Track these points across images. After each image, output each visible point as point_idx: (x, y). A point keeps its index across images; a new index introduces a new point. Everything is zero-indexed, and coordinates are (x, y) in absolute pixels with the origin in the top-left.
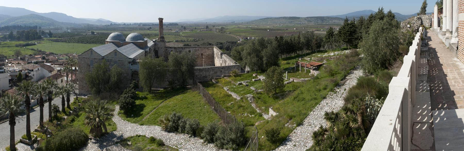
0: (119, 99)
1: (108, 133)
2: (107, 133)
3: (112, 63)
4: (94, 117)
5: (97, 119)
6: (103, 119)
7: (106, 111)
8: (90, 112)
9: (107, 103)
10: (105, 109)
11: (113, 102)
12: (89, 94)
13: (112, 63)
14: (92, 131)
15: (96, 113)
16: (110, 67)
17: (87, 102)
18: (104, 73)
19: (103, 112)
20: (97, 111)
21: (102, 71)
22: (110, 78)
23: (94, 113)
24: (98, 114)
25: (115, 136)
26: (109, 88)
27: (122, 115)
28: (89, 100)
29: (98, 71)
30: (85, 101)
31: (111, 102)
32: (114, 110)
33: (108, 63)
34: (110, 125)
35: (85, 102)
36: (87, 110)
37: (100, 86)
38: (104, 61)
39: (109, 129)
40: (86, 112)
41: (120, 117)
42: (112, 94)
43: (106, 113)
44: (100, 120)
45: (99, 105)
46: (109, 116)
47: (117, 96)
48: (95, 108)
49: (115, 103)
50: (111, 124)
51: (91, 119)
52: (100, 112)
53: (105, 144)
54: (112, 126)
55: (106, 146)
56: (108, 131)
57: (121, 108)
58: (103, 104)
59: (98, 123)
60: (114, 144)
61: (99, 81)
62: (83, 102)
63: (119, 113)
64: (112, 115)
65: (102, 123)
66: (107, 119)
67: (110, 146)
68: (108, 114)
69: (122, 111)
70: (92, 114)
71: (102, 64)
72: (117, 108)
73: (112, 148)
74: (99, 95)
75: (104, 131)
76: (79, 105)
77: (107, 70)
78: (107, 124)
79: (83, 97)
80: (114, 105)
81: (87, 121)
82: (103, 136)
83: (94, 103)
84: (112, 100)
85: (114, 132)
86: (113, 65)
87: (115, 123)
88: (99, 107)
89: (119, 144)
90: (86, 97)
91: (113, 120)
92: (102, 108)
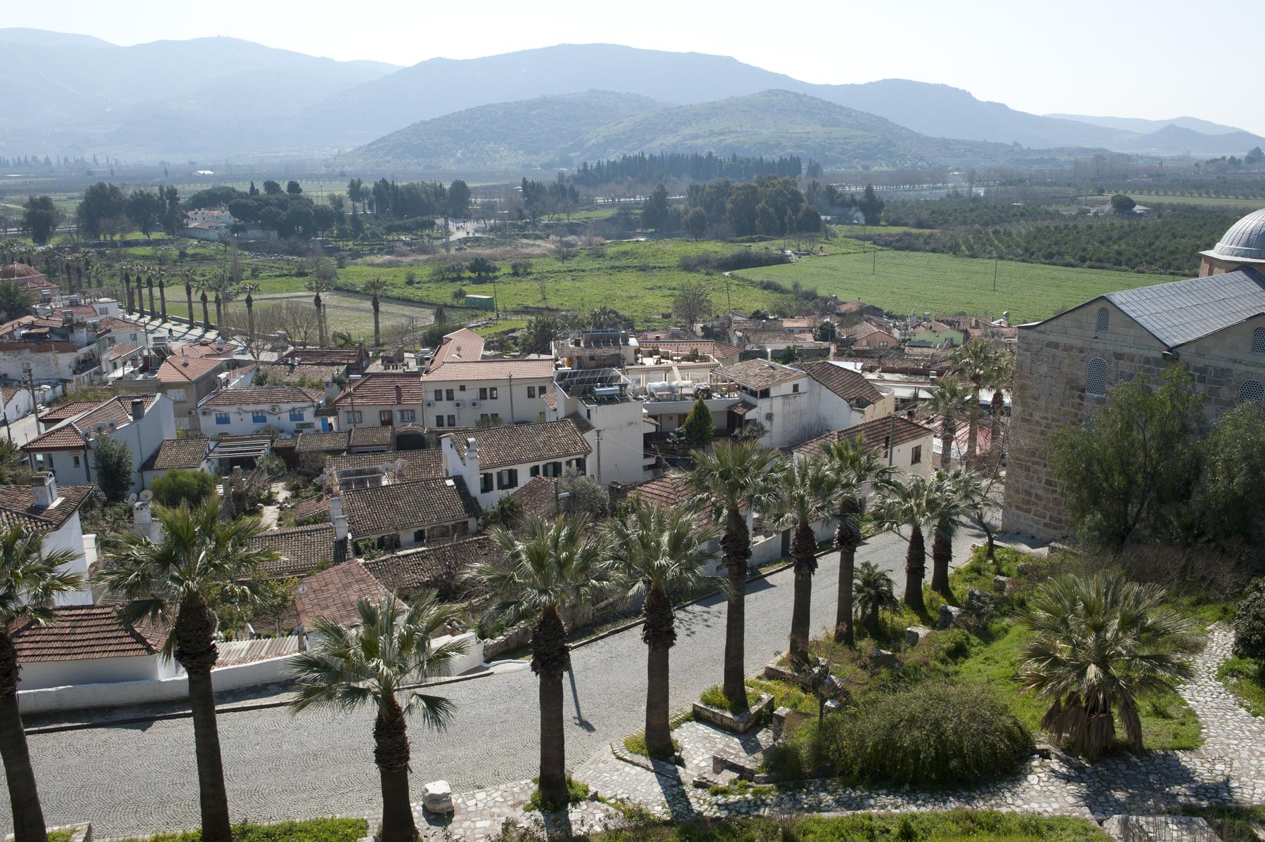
0: (1241, 594)
1: (1145, 753)
2: (1134, 746)
3: (1225, 393)
4: (1074, 653)
5: (1092, 670)
6: (1129, 679)
7: (1149, 642)
8: (1058, 626)
9: (1163, 601)
10: (1145, 629)
11: (1199, 603)
12: (1064, 539)
13: (1225, 393)
14: (1053, 720)
15: (1090, 641)
16: (1208, 410)
17: (1042, 579)
18: (1167, 440)
19: (1129, 642)
20: (1099, 629)
21: (1152, 429)
22: (1198, 471)
23: (1076, 637)
24: (1102, 645)
25: (1185, 776)
26: (1188, 528)
27: (1246, 683)
28: (1053, 569)
29: (1129, 426)
30: (1036, 568)
31: (1185, 601)
32: (1196, 648)
33: (1201, 388)
34: (1160, 713)
35: (1032, 573)
36: (1041, 614)
37: (1132, 510)
38: (1174, 371)
39: (1154, 733)
40: (1034, 624)
41: (1234, 690)
42: (1200, 564)
43: (1146, 652)
44: (1109, 680)
45: (1115, 602)
46: (1164, 666)
47: (1227, 579)
48: (1089, 610)
49: (1208, 612)
50: (1171, 710)
51: (1056, 662)
52: (1117, 640)
53: (1119, 795)
54: (1173, 726)
55: (1120, 808)
56: (1148, 742)
57: (1246, 647)
58: (1138, 602)
59: (1093, 690)
60: (1171, 813)
61: (1131, 481)
62: (1021, 572)
63: (1226, 672)
64: (1185, 671)
65: (1115, 693)
66: (1149, 682)
67: (1146, 812)
68: (1161, 660)
69: (1251, 666)
70: (1068, 639)
71: (1158, 390)
72: (1221, 642)
73: (1157, 826)
74: (1118, 551)
75: (1121, 734)
76: (1000, 587)
77: (1185, 429)
78: (1143, 705)
79: (1024, 548)
80: (1203, 621)
81: (1032, 666)
82: (1115, 759)
83: (1089, 588)
84: (1199, 592)
85: (1184, 758)
86: (1230, 404)
87: (1191, 712)
88: (1108, 613)
89: (1201, 821)
90: (1044, 551)
91: (1186, 696)
92: (1129, 623)
